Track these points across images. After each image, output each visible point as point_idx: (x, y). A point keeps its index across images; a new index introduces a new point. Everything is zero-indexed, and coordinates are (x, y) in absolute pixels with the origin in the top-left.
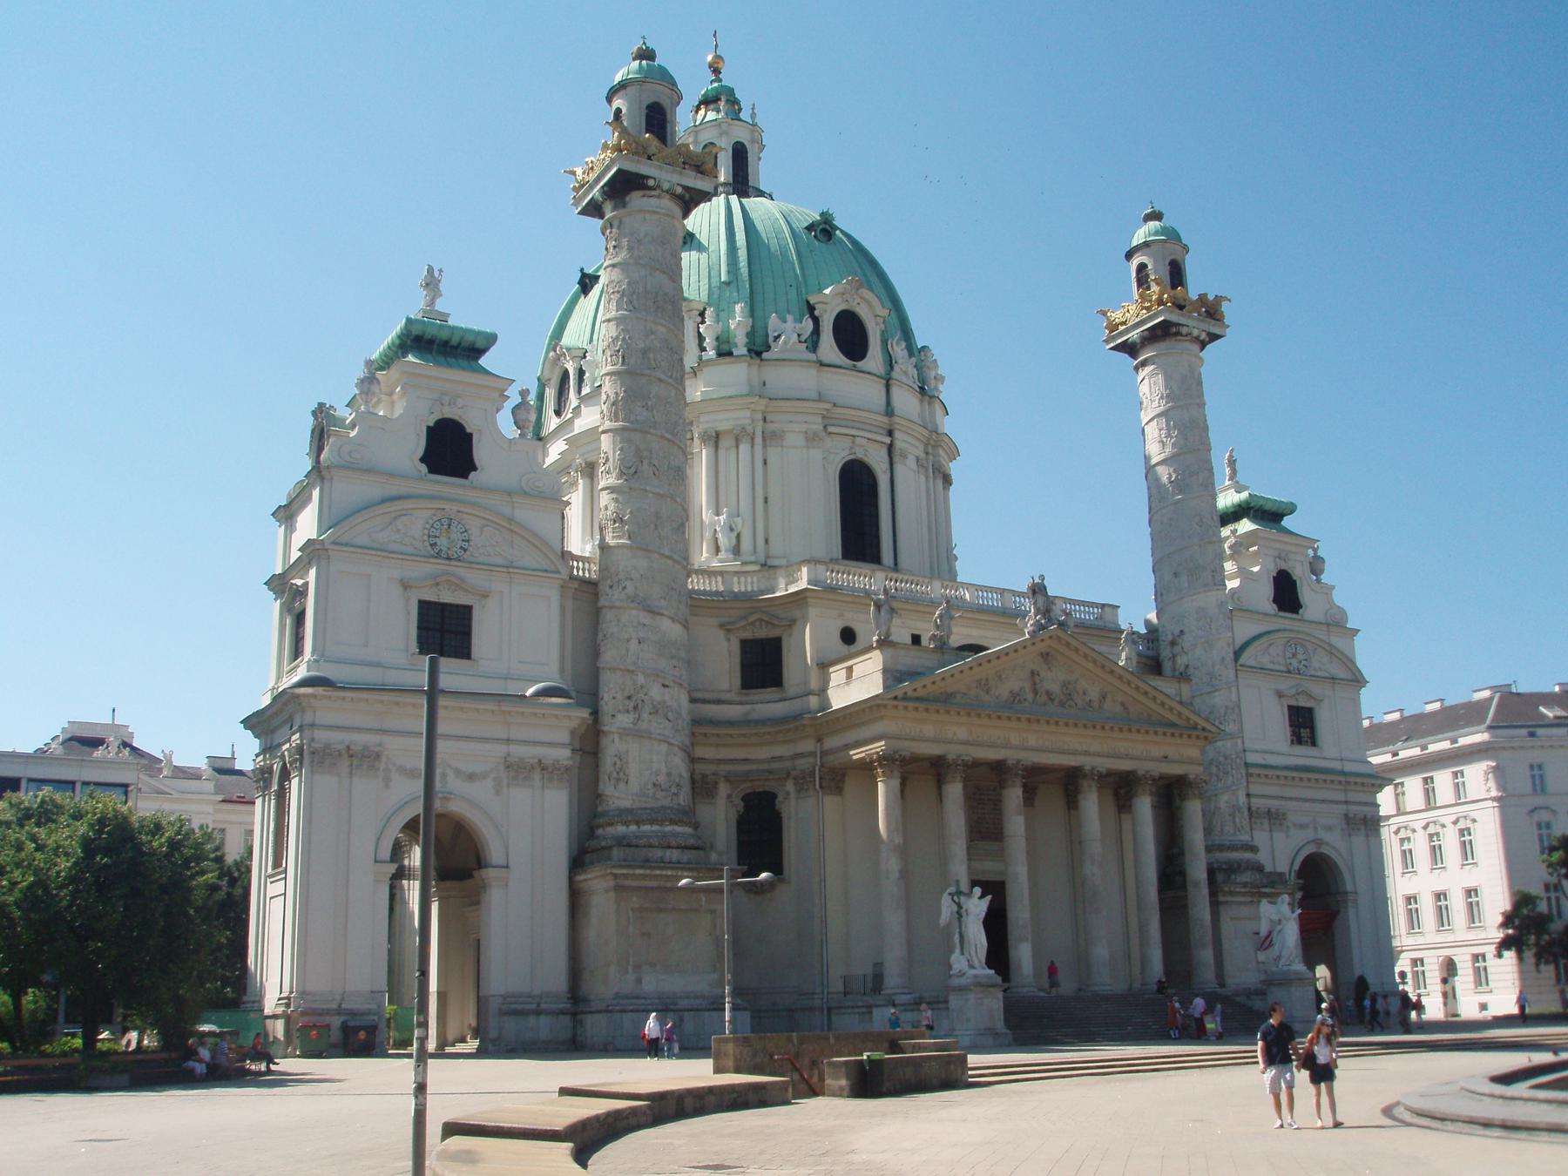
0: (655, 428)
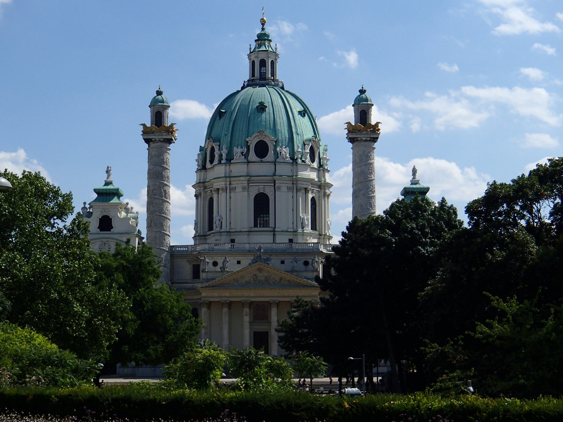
0: (155, 212)
